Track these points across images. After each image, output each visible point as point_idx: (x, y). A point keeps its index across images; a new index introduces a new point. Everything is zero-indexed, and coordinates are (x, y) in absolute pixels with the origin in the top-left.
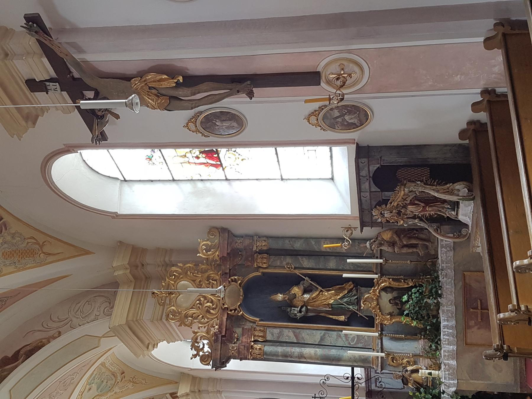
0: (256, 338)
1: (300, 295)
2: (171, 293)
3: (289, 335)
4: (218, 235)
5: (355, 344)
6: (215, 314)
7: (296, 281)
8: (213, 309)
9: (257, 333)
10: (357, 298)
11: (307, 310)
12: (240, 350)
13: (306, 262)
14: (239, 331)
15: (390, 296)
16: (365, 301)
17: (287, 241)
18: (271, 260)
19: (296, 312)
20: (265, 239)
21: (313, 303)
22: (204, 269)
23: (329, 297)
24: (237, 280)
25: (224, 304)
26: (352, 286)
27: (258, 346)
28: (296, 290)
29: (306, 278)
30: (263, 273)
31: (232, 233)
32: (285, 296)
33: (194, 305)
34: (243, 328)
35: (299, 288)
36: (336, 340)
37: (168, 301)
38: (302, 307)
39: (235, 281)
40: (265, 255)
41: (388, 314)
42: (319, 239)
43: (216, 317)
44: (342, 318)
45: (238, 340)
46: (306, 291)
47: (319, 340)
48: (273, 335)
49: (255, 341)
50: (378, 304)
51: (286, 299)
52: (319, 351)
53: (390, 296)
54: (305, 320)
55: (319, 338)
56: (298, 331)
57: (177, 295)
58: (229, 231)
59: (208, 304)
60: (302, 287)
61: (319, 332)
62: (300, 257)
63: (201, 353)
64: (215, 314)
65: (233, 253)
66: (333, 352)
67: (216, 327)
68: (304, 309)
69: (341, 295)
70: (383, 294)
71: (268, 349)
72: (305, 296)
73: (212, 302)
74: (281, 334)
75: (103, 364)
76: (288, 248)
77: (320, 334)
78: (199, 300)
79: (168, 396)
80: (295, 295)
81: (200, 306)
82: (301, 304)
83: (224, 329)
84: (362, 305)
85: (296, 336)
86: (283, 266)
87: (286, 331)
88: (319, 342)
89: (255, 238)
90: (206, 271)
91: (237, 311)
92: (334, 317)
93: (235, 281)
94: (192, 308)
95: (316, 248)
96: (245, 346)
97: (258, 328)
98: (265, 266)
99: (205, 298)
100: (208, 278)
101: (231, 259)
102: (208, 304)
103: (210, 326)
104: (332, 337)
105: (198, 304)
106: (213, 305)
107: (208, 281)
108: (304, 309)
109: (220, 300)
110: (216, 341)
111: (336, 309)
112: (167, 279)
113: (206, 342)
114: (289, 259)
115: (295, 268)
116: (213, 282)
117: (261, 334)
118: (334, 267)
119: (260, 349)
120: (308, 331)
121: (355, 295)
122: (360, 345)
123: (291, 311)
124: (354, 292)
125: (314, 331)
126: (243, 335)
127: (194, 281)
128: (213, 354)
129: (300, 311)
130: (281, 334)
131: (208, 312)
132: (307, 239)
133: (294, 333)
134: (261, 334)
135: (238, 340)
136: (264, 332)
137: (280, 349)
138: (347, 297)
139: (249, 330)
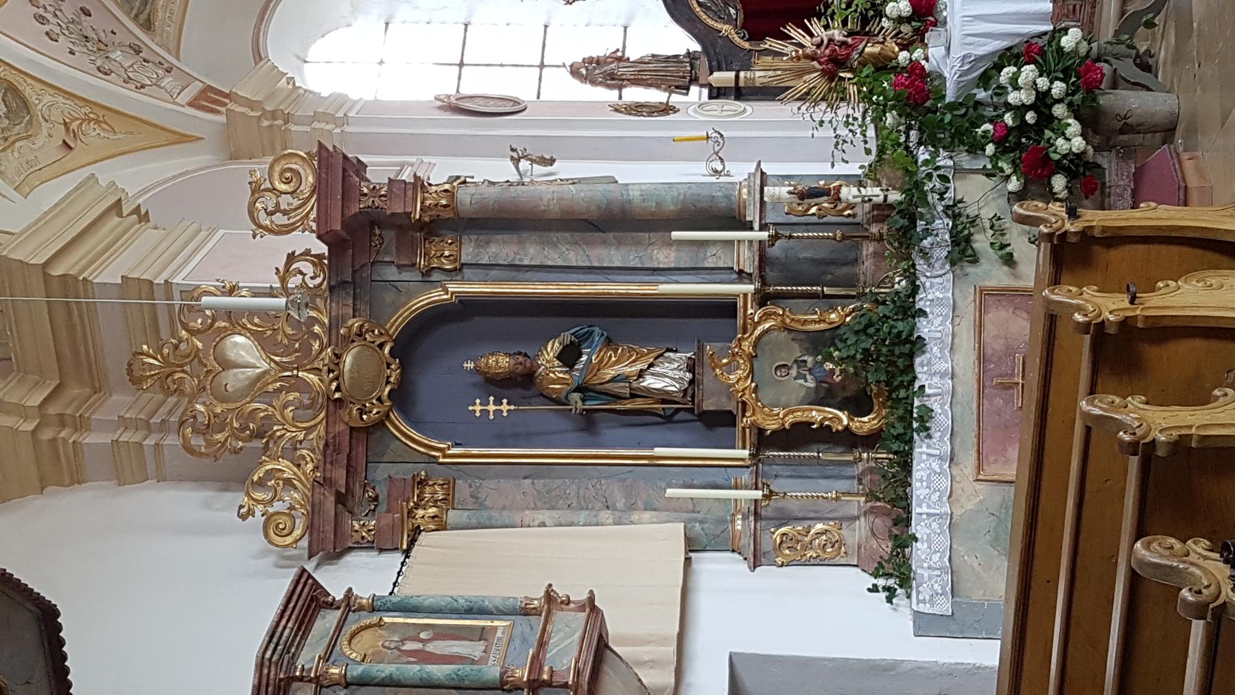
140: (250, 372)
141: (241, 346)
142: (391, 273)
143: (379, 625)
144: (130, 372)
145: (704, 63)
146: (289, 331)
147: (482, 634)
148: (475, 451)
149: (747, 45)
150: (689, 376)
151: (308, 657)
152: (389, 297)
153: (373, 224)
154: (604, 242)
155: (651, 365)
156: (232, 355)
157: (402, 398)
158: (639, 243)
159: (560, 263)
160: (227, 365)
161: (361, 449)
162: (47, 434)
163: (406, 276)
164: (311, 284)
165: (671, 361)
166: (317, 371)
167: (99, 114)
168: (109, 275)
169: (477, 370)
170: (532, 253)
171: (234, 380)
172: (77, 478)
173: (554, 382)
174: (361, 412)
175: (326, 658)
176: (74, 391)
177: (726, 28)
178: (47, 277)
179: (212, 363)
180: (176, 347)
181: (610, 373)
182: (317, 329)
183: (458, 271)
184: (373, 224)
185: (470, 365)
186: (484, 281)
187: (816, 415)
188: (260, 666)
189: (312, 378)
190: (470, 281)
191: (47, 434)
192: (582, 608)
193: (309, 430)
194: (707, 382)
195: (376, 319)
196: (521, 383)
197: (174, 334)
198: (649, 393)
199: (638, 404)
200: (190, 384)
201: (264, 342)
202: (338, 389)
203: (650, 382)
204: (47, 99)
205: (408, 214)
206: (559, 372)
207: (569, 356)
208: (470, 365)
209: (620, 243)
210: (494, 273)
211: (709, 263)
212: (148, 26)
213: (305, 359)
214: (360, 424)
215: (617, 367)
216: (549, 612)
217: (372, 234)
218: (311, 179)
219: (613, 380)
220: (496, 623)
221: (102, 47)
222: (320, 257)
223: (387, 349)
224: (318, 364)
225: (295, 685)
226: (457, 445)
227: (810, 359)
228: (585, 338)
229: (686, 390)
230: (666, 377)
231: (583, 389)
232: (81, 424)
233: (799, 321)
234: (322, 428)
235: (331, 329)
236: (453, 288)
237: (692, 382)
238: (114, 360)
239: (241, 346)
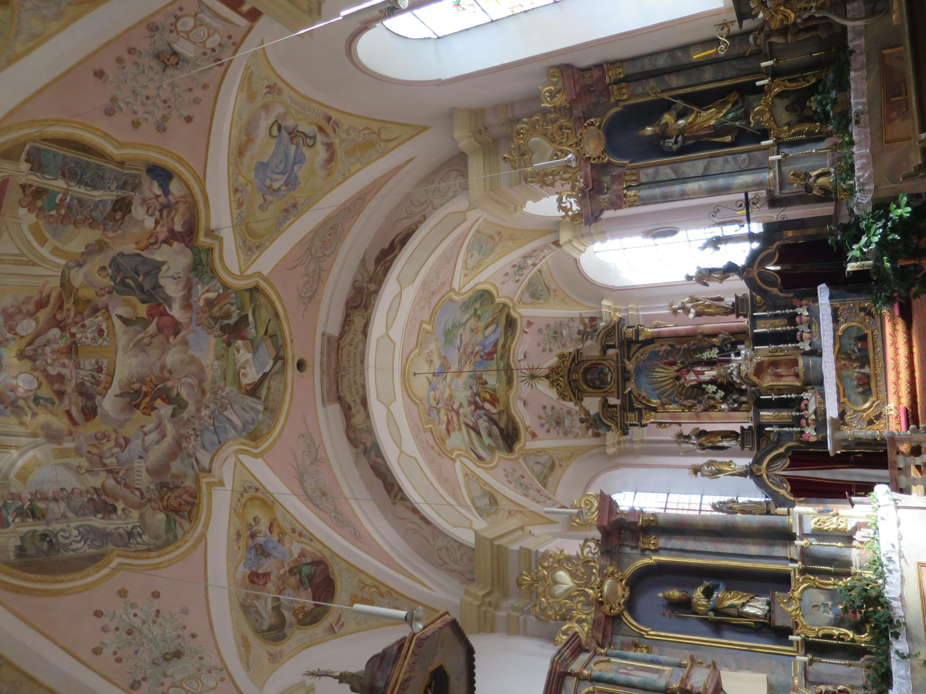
0: (629, 184)
3: (666, 172)
7: (666, 106)
9: (627, 178)
11: (685, 139)
13: (675, 81)
14: (607, 179)
15: (786, 102)
17: (646, 61)
23: (709, 117)
26: (737, 96)
27: (632, 193)
28: (667, 118)
29: (678, 101)
30: (625, 107)
34: (612, 176)
35: (670, 115)
38: (677, 137)
39: (592, 124)
40: (624, 84)
41: (785, 125)
42: (685, 48)
44: (728, 139)
45: (608, 189)
46: (680, 116)
48: (647, 175)
49: (629, 188)
50: (772, 116)
52: (704, 184)
53: (786, 102)
54: (684, 150)
56: (676, 165)
62: (666, 77)
63: (570, 213)
65: (586, 91)
66: (721, 182)
68: (680, 138)
69: (725, 111)
70: (778, 101)
71: (644, 193)
72: (681, 122)
74: (656, 173)
75: (478, 231)
80: (666, 124)
82: (675, 133)
84: (752, 121)
85: (675, 172)
93: (592, 124)
97: (628, 172)
98: (625, 97)
104: (718, 164)
108: (680, 138)
110: (584, 197)
111: (719, 130)
113: (572, 200)
114: (652, 83)
115: (662, 91)
117: (634, 178)
118: (711, 79)
120: (688, 163)
121: (741, 108)
122: (753, 166)
124: (740, 104)
126: (613, 183)
129: (676, 142)
130: (656, 173)
134: (634, 178)
135: (608, 189)
136: (638, 175)
137: (657, 191)
139: (619, 176)
140: (565, 587)
141: (562, 575)
142: (628, 550)
143: (608, 661)
144: (517, 581)
145: (772, 506)
146: (583, 570)
147: (657, 671)
148: (662, 634)
149: (792, 498)
150: (767, 608)
151: (575, 667)
152: (626, 560)
153: (621, 528)
154: (724, 542)
155: (748, 601)
156: (558, 580)
157: (630, 605)
158: (741, 543)
159: (703, 549)
160: (556, 583)
161: (610, 627)
162: (483, 609)
163: (634, 551)
164: (593, 551)
165: (758, 601)
166: (592, 588)
167: (522, 510)
168: (516, 547)
169: (665, 598)
170: (690, 544)
171: (559, 590)
172: (492, 631)
173: (702, 605)
174: (611, 608)
175: (585, 666)
176: (496, 595)
177: (782, 492)
178: (492, 545)
179: (550, 582)
180: (537, 573)
181: (727, 603)
182: (594, 571)
183: (656, 551)
184: (621, 528)
185: (661, 595)
186: (669, 556)
187: (835, 632)
188: (553, 662)
189: (591, 591)
190: (662, 556)
191: (483, 609)
192: (709, 667)
193: (587, 614)
194: (777, 612)
195: (620, 567)
196: (685, 605)
197: (537, 568)
198: (748, 616)
199: (743, 621)
200: (541, 589)
201: (573, 576)
202: (601, 597)
203: (747, 609)
204: (504, 502)
205: (636, 523)
206: (704, 602)
207: (708, 593)
208: (661, 595)
209: (732, 542)
210: (673, 553)
211: (776, 554)
212: (544, 486)
213: (588, 584)
214: (609, 614)
215: (732, 600)
216: (692, 666)
217: (620, 533)
218: (596, 504)
219: (730, 606)
220: (665, 668)
221: (527, 488)
222: (598, 541)
223: (624, 582)
224: (593, 586)
225: (568, 677)
226: (653, 630)
227: (830, 603)
228: (716, 587)
229: (766, 615)
230: (756, 608)
231: (716, 611)
232: (497, 607)
233: (822, 584)
234: (593, 614)
235: (600, 571)
236: (654, 558)
237: (769, 611)
238: (512, 576)
239: (562, 575)
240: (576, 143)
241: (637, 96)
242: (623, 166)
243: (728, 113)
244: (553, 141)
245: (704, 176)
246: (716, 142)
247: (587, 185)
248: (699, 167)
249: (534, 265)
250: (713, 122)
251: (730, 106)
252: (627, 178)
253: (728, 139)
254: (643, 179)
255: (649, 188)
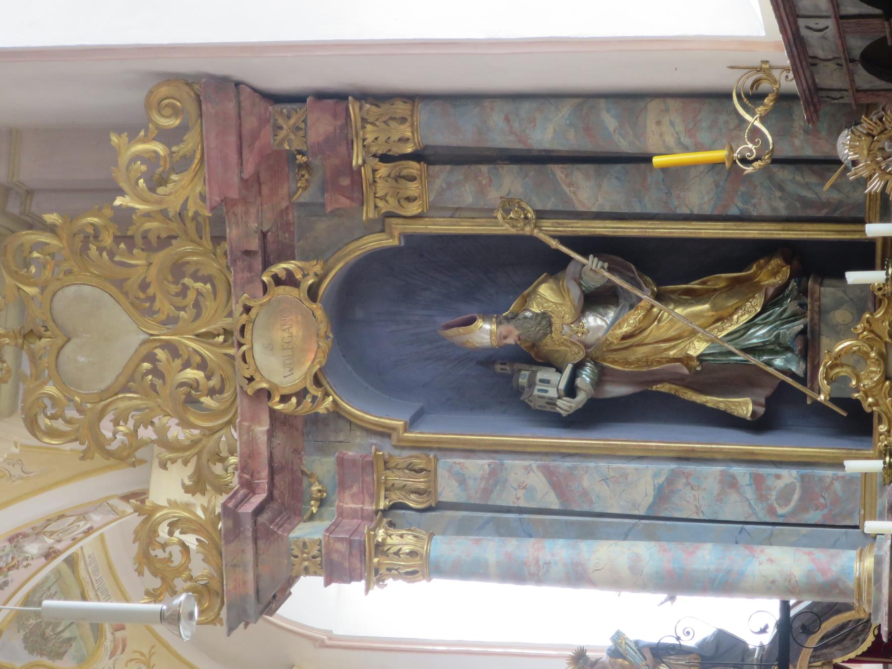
0: (396, 497)
1: (568, 318)
2: (30, 335)
3: (527, 481)
4: (192, 108)
5: (794, 513)
6: (223, 412)
7: (553, 264)
8: (212, 392)
9: (395, 478)
10: (803, 332)
11: (602, 376)
12: (335, 557)
13: (587, 191)
14: (322, 467)
16: (832, 367)
18: (439, 183)
19: (552, 393)
20: (401, 108)
21: (624, 354)
22: (153, 238)
23: (688, 329)
24: (299, 276)
25: (251, 379)
26: (786, 271)
27: (401, 540)
28: (547, 296)
29: (592, 262)
30: (409, 238)
31: (255, 90)
32: (505, 328)
33: (132, 378)
34: (341, 462)
35: (561, 292)
36: (720, 498)
37: (26, 367)
39: (290, 280)
40: (413, 167)
42: (631, 100)
43: (230, 423)
44: (744, 406)
45: (322, 502)
46: (596, 299)
47: (650, 499)
48: (462, 481)
51: (511, 341)
52: (646, 553)
54: (596, 414)
55: (651, 492)
56: (565, 464)
57: (60, 341)
58: (237, 84)
59: (191, 374)
60: (576, 293)
61: (650, 468)
62: (558, 171)
64: (223, 412)
67: (233, 460)
68: (586, 377)
69: (741, 319)
72: (593, 321)
73: (203, 365)
74: (495, 477)
76: (504, 145)
77: (656, 475)
78: (151, 357)
79: (116, 502)
80: (545, 318)
81: (158, 382)
83: (265, 473)
84: (823, 383)
85: (557, 485)
86: (487, 208)
87: (515, 466)
88: (651, 507)
89: (353, 108)
90: (165, 242)
91: (309, 399)
92: (711, 401)
93: (290, 280)
94: (125, 389)
95: (624, 145)
96: (350, 543)
97: (402, 457)
98: (413, 209)
99: (173, 350)
100: (178, 270)
101: (265, 190)
102: (191, 374)
103: (205, 457)
105: (148, 372)
106: (208, 378)
107: (176, 283)
108: (586, 377)
109: (232, 357)
110: (234, 533)
111: (715, 375)
112: (8, 280)
113: (191, 540)
114: (510, 181)
115: (541, 215)
116: (199, 285)
117: (420, 482)
118: (707, 210)
119: (412, 554)
120: (603, 464)
121: (795, 317)
122: (814, 516)
123: (532, 384)
125: (631, 466)
126: (342, 485)
127: (120, 284)
128: (229, 585)
129: (571, 390)
130: (495, 477)
131: (191, 401)
132: (587, 100)
133: (549, 473)
134: (420, 482)
135: (322, 502)
138: (766, 324)
139: (369, 465)
240: (227, 333)
241: (456, 212)
242: (385, 433)
243: (750, 324)
244: (141, 304)
245: (654, 520)
246: (702, 407)
247: (250, 487)
248: (641, 483)
249: (50, 555)
250: (697, 348)
251: (756, 304)
252: (395, 478)
253: (744, 406)
254: (448, 491)
255: (463, 529)
